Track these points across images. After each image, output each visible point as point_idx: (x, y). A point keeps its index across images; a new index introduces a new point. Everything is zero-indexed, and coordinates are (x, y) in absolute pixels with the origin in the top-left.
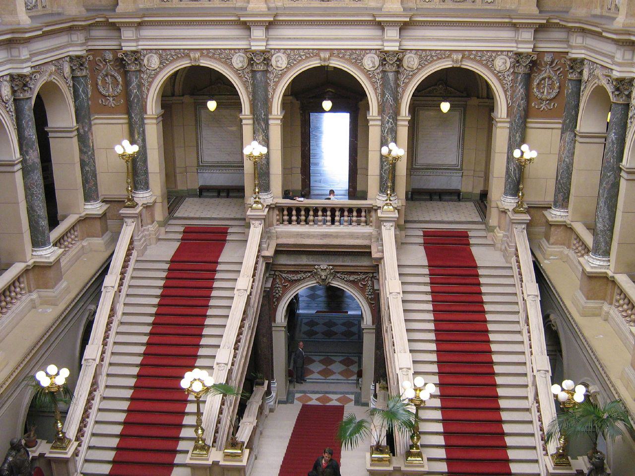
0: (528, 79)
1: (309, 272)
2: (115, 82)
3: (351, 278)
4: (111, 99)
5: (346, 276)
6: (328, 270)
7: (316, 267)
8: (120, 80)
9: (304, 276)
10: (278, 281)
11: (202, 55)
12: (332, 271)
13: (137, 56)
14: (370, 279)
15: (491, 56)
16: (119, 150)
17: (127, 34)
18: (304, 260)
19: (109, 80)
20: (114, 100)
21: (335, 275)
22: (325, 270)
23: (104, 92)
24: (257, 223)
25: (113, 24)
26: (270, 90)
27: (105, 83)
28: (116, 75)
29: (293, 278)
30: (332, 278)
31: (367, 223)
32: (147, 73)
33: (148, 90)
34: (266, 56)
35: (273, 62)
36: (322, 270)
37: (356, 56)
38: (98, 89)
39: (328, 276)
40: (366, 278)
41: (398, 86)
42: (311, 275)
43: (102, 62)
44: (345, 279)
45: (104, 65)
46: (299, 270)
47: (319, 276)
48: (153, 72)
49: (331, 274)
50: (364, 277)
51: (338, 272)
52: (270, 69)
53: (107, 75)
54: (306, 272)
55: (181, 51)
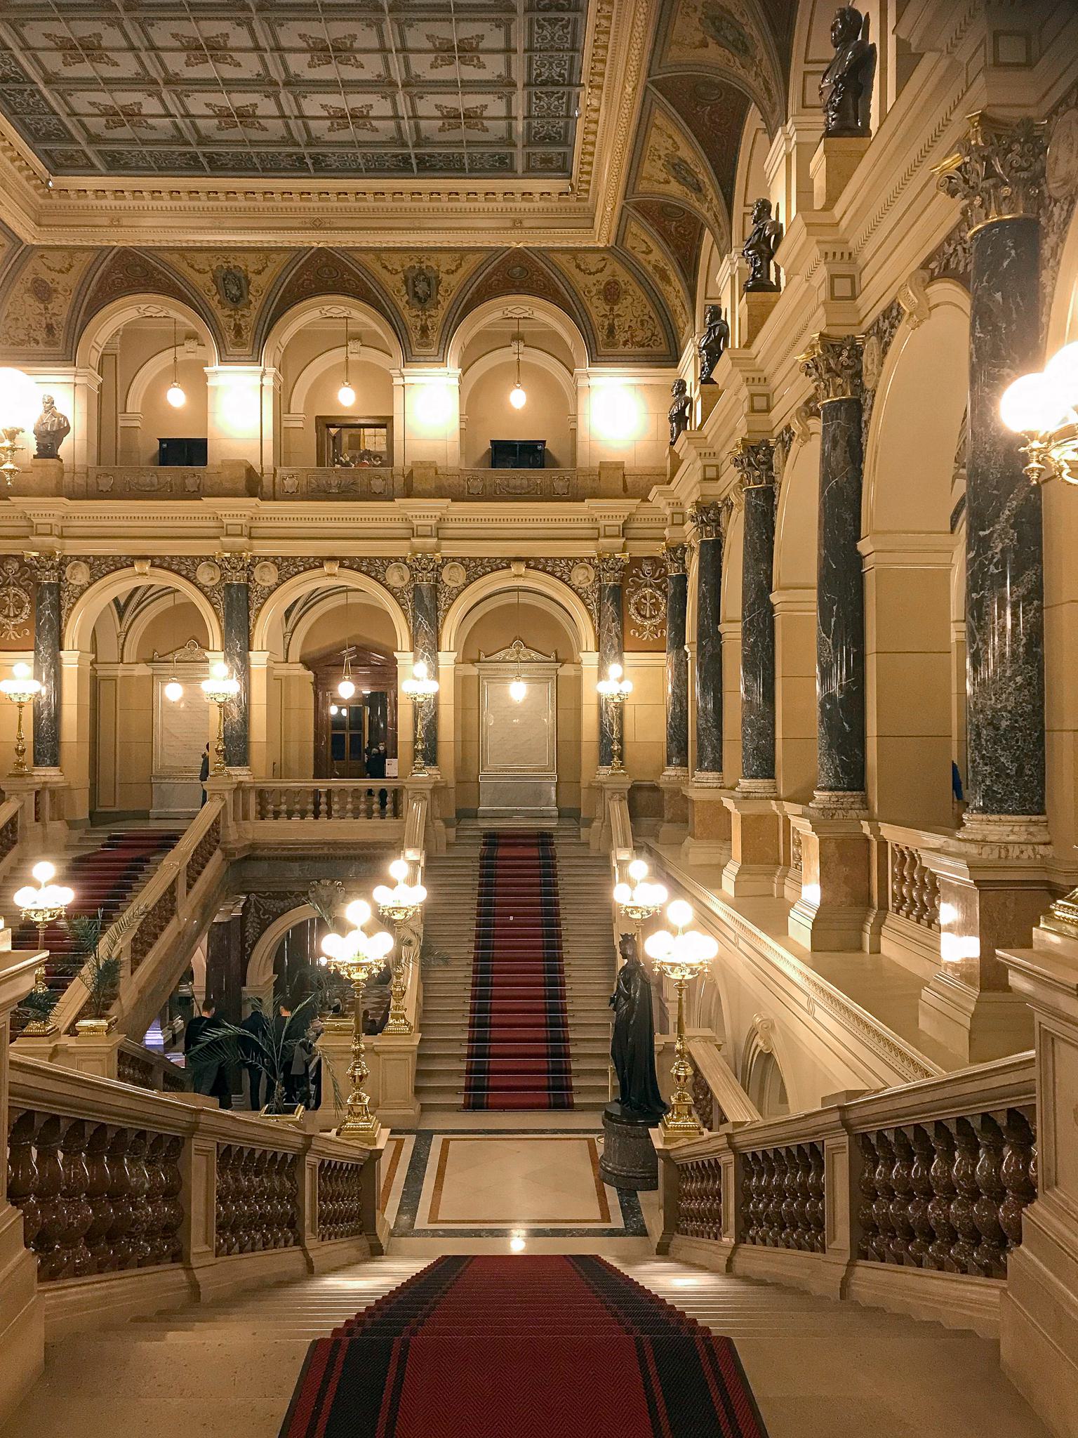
0: (618, 595)
15: (567, 565)
26: (252, 613)
41: (437, 609)
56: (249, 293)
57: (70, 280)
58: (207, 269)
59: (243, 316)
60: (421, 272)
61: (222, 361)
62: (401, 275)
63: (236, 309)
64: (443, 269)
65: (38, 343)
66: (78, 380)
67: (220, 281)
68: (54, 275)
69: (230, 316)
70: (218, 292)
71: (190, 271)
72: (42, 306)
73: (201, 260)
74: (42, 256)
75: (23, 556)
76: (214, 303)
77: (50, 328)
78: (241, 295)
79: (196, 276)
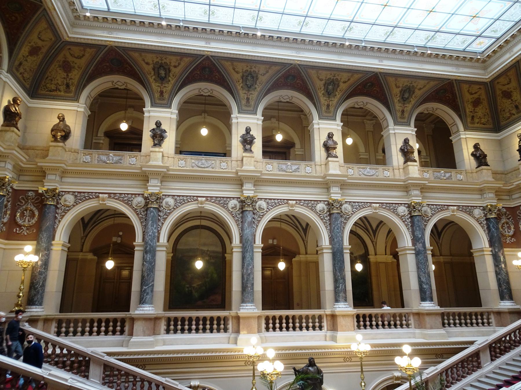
2: (33, 215)
4: (25, 229)
8: (37, 213)
11: (110, 197)
13: (56, 195)
16: (19, 258)
17: (50, 177)
19: (27, 213)
20: (27, 229)
23: (20, 222)
25: (41, 167)
27: (22, 215)
28: (34, 209)
32: (61, 209)
33: (60, 221)
34: (159, 198)
35: (164, 204)
37: (222, 202)
38: (15, 220)
43: (24, 200)
45: (26, 202)
48: (67, 208)
52: (161, 209)
53: (26, 210)
55: (94, 194)
56: (169, 76)
57: (83, 62)
58: (151, 62)
59: (165, 87)
60: (250, 73)
61: (152, 106)
62: (241, 74)
63: (162, 83)
64: (260, 73)
65: (60, 91)
66: (79, 109)
67: (156, 70)
68: (74, 59)
69: (158, 86)
70: (154, 75)
71: (142, 62)
72: (65, 74)
73: (149, 58)
74: (70, 49)
75: (38, 191)
76: (151, 80)
77: (68, 86)
78: (165, 77)
79: (144, 65)
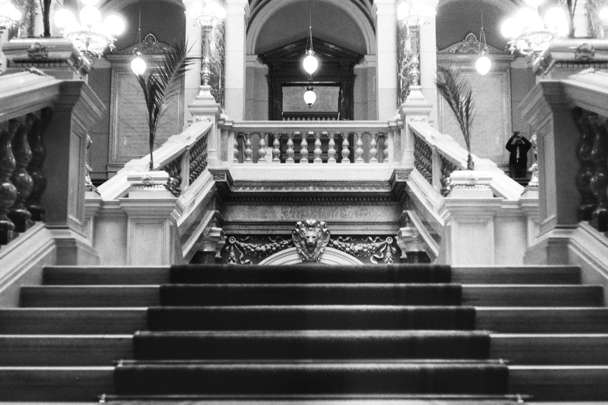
1: (288, 237)
3: (358, 247)
5: (348, 244)
6: (317, 230)
7: (299, 223)
9: (278, 245)
10: (232, 254)
12: (325, 230)
14: (389, 248)
18: (278, 214)
21: (330, 242)
22: (313, 226)
24: (203, 117)
29: (258, 248)
30: (324, 245)
31: (382, 157)
36: (308, 226)
39: (319, 241)
40: (381, 247)
42: (289, 244)
44: (348, 249)
46: (270, 232)
47: (303, 242)
49: (325, 235)
50: (378, 245)
51: (334, 237)
54: (279, 238)
